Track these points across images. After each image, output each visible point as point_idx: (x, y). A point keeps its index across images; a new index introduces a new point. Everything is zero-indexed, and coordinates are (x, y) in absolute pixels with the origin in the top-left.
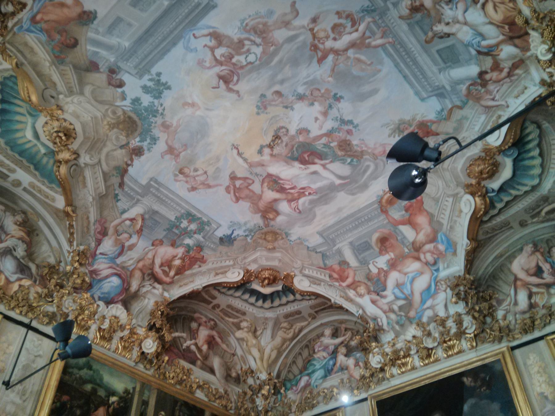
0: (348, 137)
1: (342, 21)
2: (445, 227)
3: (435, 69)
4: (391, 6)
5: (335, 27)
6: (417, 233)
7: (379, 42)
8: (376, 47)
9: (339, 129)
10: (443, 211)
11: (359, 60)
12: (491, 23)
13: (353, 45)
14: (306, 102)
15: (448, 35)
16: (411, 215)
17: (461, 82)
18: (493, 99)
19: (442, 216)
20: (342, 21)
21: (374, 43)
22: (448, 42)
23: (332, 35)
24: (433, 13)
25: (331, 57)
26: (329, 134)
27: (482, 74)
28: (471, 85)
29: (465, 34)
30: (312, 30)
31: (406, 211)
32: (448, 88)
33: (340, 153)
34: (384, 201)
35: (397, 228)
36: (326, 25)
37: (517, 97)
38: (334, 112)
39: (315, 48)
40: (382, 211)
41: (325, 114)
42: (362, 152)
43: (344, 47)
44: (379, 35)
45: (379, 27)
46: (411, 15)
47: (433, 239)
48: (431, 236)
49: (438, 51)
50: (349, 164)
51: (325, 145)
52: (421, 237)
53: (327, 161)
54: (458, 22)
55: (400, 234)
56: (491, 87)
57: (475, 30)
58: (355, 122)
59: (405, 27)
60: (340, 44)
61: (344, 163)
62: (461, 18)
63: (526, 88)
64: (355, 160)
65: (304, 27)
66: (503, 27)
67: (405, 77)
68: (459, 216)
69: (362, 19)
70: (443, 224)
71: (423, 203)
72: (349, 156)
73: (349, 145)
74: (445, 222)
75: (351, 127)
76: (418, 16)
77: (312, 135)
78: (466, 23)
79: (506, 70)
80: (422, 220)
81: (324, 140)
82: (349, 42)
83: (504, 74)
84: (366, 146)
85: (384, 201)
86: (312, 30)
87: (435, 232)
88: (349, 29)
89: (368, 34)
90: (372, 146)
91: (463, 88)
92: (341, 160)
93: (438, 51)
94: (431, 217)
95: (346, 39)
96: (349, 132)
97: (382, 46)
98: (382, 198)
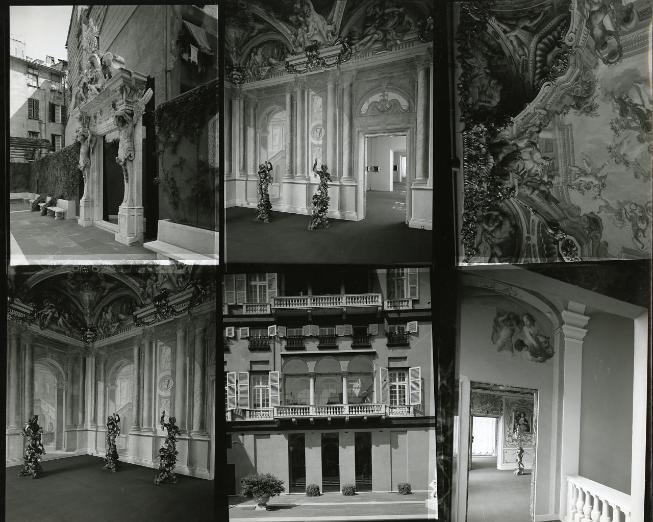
0: (619, 118)
1: (583, 188)
2: (585, 24)
3: (558, 142)
4: (561, 184)
5: (589, 189)
6: (602, 21)
7: (574, 169)
8: (577, 167)
9: (622, 127)
10: (585, 36)
11: (589, 165)
12: (523, 160)
13: (586, 174)
14: (626, 158)
15: (544, 158)
16: (604, 39)
17: (550, 130)
18: (540, 113)
19: (586, 33)
20: (583, 188)
21: (577, 169)
22: (545, 155)
23: (592, 185)
24: (546, 172)
25: (599, 175)
26: (628, 127)
27: (539, 132)
28: (546, 126)
29: (537, 156)
30: (599, 195)
31: (606, 43)
32: (557, 128)
33: (629, 108)
34: (618, 56)
35: (615, 29)
36: (593, 192)
37: (529, 113)
38: (618, 141)
39: (604, 185)
40: (621, 49)
41: (622, 143)
42: (617, 102)
43: (590, 176)
44: (574, 172)
45: (571, 177)
46: (555, 176)
47: (592, 13)
48: (593, 17)
49: (552, 151)
50: (628, 97)
51: (634, 120)
52: (600, 17)
53: (639, 107)
54: (537, 164)
55: (614, 23)
56: (538, 122)
57: (532, 157)
58: (610, 127)
59: (560, 170)
60: (591, 179)
61: (631, 100)
62: (536, 165)
63: (523, 119)
64: (624, 98)
65: (602, 199)
66: (519, 157)
67: (573, 143)
68: (576, 30)
69: (575, 185)
70: (586, 26)
71: (595, 46)
72: (625, 103)
73: (622, 112)
74: (584, 27)
75: (614, 124)
76: (552, 173)
77: (637, 133)
78: (535, 162)
79: (528, 132)
80: (598, 32)
81: (634, 125)
82: (587, 177)
83: (529, 129)
84: (613, 105)
85: (618, 56)
86: (599, 195)
87: (589, 21)
88: (583, 183)
89: (577, 176)
90: (610, 103)
91: (550, 125)
92: (630, 103)
93: (552, 151)
94: (592, 35)
95: (587, 180)
96: (617, 121)
97: (574, 166)
98: (618, 59)
